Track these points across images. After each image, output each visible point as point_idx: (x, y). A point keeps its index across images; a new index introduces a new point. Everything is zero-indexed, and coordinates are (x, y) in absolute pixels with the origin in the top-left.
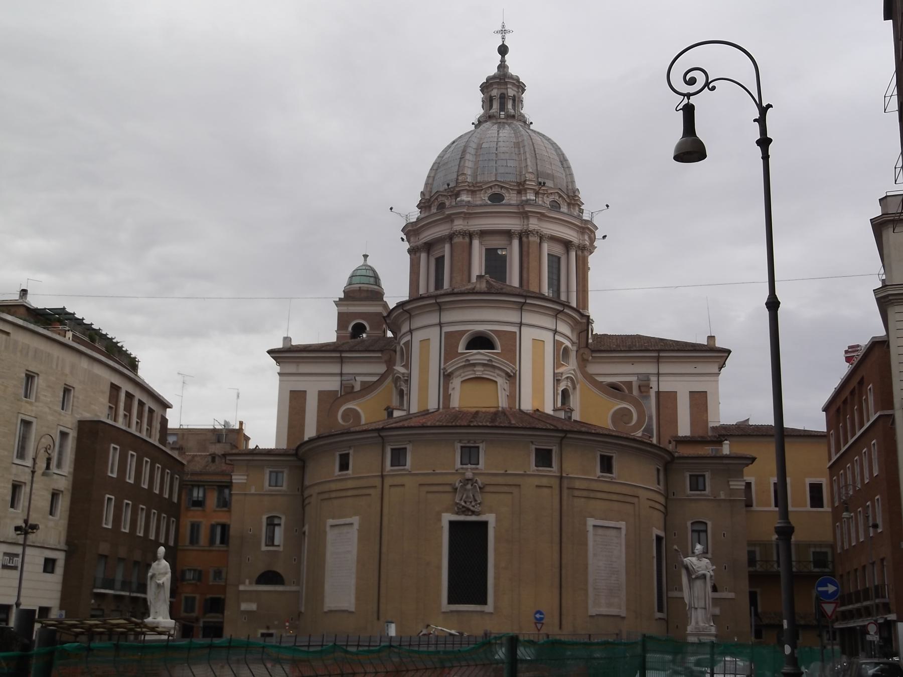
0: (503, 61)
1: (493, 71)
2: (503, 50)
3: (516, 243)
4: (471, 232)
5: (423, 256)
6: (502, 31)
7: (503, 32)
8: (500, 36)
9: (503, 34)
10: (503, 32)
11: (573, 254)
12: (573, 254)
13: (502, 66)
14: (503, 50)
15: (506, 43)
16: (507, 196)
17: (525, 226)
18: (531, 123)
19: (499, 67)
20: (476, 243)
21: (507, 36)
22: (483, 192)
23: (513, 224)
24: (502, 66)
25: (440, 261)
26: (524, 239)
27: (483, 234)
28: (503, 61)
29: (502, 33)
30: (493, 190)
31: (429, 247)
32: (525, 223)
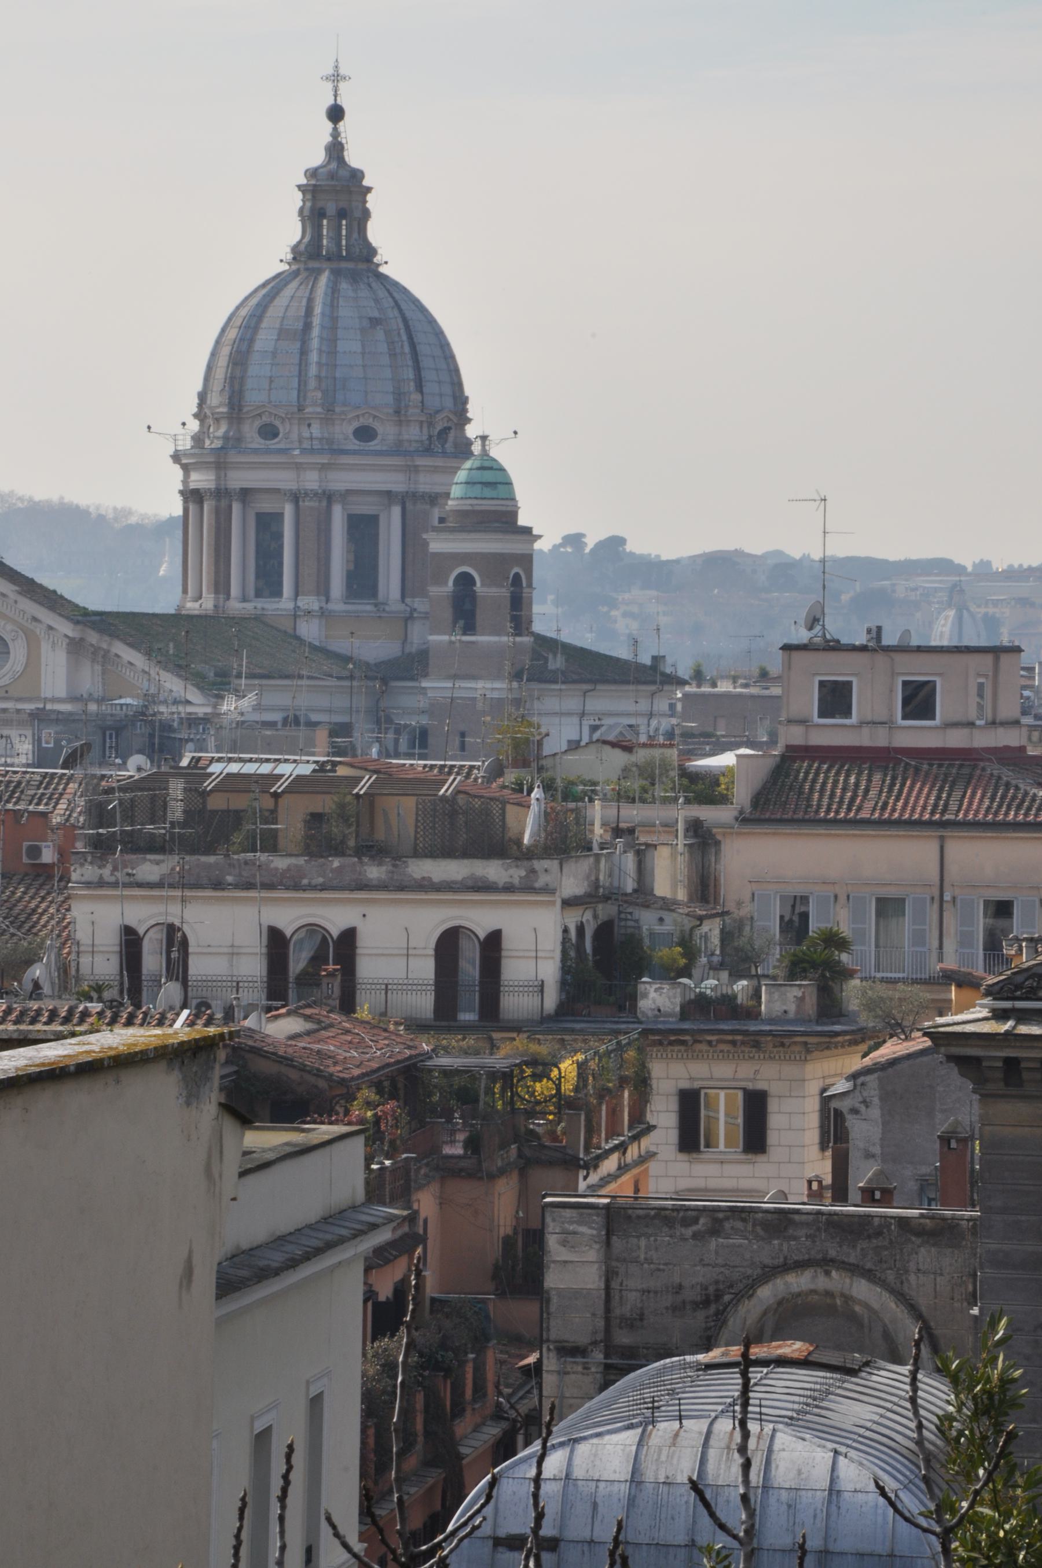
1: (317, 158)
2: (336, 114)
8: (329, 86)
13: (336, 149)
14: (336, 114)
15: (339, 102)
21: (342, 85)
24: (336, 149)
28: (335, 134)
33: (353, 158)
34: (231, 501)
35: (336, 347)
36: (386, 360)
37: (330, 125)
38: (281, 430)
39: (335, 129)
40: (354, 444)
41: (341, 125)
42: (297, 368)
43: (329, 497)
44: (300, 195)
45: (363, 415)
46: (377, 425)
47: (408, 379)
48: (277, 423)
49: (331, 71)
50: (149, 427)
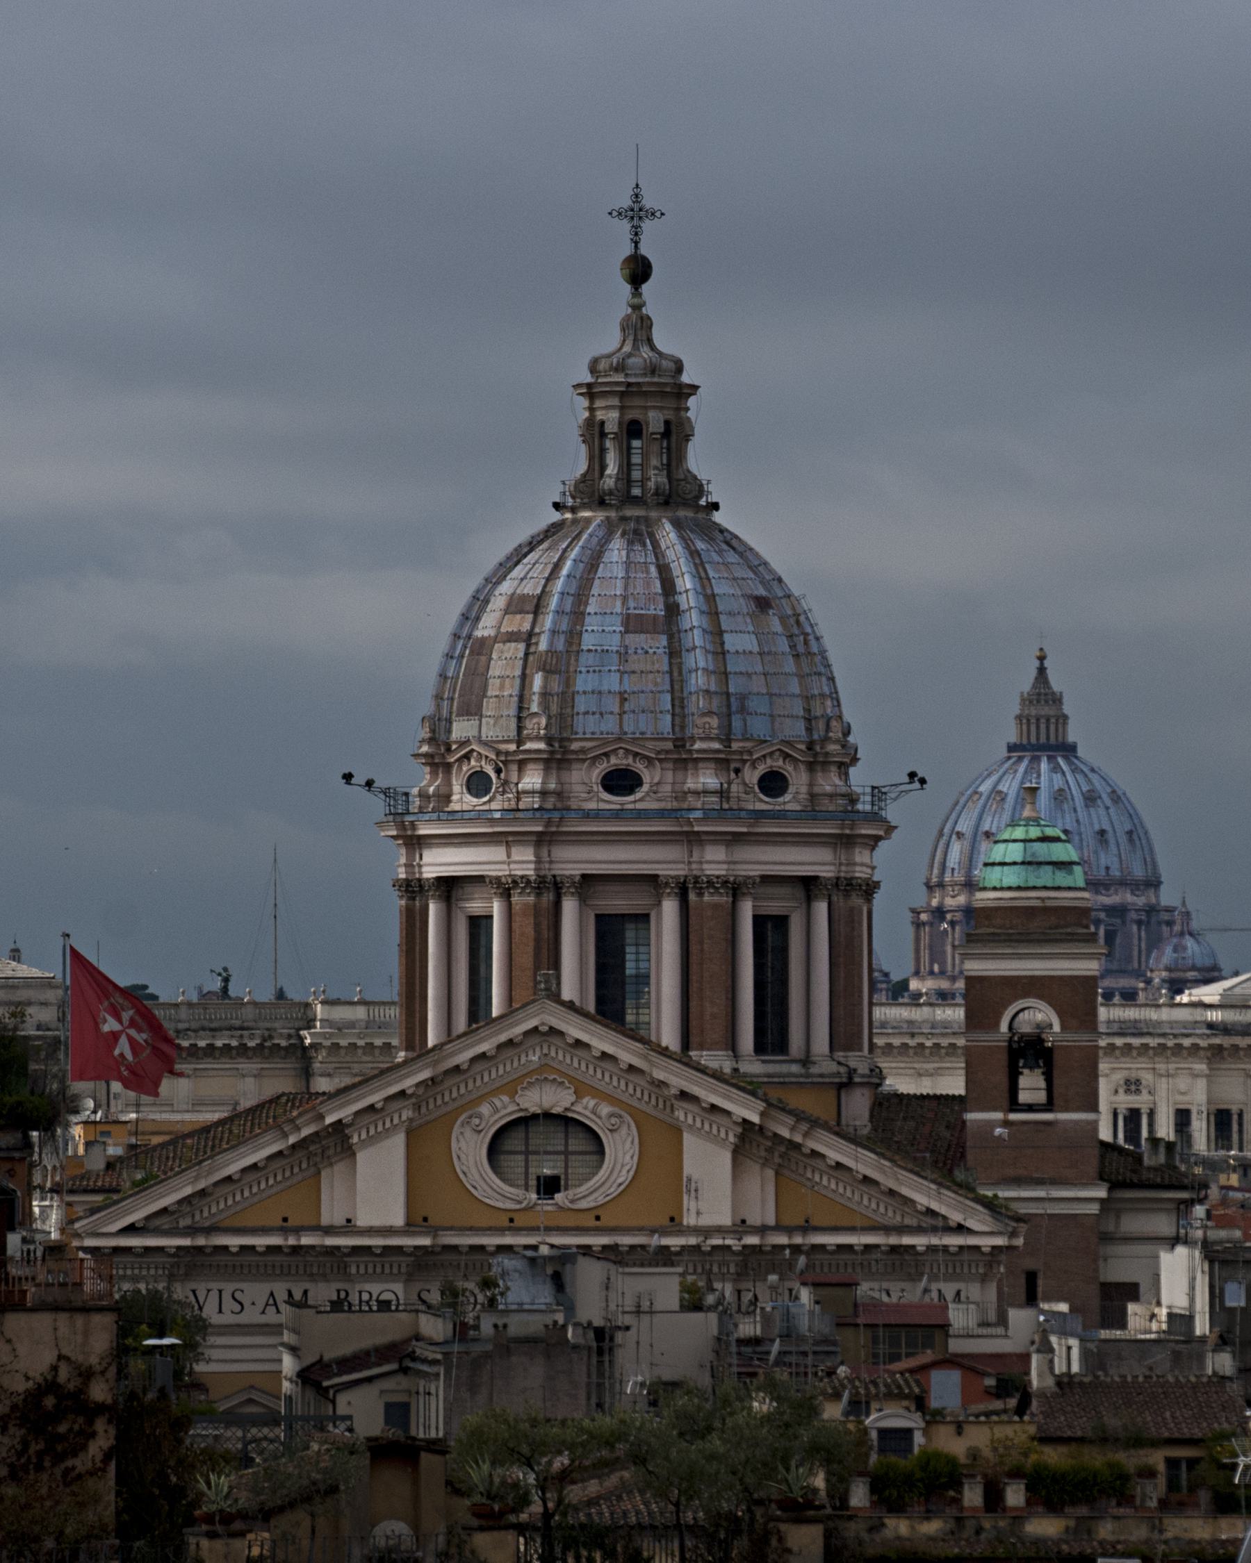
3: (670, 908)
4: (558, 879)
5: (434, 910)
7: (637, 213)
8: (625, 226)
9: (636, 207)
11: (821, 909)
12: (821, 908)
14: (638, 271)
15: (644, 250)
16: (648, 777)
17: (694, 866)
18: (716, 506)
20: (569, 907)
21: (647, 225)
22: (586, 764)
25: (479, 925)
26: (692, 897)
27: (588, 882)
28: (637, 308)
30: (613, 760)
31: (449, 887)
32: (695, 858)
35: (723, 644)
36: (790, 665)
37: (627, 288)
38: (646, 777)
40: (764, 803)
41: (645, 288)
42: (667, 677)
43: (736, 889)
45: (771, 754)
46: (788, 769)
47: (822, 695)
48: (639, 767)
50: (348, 777)
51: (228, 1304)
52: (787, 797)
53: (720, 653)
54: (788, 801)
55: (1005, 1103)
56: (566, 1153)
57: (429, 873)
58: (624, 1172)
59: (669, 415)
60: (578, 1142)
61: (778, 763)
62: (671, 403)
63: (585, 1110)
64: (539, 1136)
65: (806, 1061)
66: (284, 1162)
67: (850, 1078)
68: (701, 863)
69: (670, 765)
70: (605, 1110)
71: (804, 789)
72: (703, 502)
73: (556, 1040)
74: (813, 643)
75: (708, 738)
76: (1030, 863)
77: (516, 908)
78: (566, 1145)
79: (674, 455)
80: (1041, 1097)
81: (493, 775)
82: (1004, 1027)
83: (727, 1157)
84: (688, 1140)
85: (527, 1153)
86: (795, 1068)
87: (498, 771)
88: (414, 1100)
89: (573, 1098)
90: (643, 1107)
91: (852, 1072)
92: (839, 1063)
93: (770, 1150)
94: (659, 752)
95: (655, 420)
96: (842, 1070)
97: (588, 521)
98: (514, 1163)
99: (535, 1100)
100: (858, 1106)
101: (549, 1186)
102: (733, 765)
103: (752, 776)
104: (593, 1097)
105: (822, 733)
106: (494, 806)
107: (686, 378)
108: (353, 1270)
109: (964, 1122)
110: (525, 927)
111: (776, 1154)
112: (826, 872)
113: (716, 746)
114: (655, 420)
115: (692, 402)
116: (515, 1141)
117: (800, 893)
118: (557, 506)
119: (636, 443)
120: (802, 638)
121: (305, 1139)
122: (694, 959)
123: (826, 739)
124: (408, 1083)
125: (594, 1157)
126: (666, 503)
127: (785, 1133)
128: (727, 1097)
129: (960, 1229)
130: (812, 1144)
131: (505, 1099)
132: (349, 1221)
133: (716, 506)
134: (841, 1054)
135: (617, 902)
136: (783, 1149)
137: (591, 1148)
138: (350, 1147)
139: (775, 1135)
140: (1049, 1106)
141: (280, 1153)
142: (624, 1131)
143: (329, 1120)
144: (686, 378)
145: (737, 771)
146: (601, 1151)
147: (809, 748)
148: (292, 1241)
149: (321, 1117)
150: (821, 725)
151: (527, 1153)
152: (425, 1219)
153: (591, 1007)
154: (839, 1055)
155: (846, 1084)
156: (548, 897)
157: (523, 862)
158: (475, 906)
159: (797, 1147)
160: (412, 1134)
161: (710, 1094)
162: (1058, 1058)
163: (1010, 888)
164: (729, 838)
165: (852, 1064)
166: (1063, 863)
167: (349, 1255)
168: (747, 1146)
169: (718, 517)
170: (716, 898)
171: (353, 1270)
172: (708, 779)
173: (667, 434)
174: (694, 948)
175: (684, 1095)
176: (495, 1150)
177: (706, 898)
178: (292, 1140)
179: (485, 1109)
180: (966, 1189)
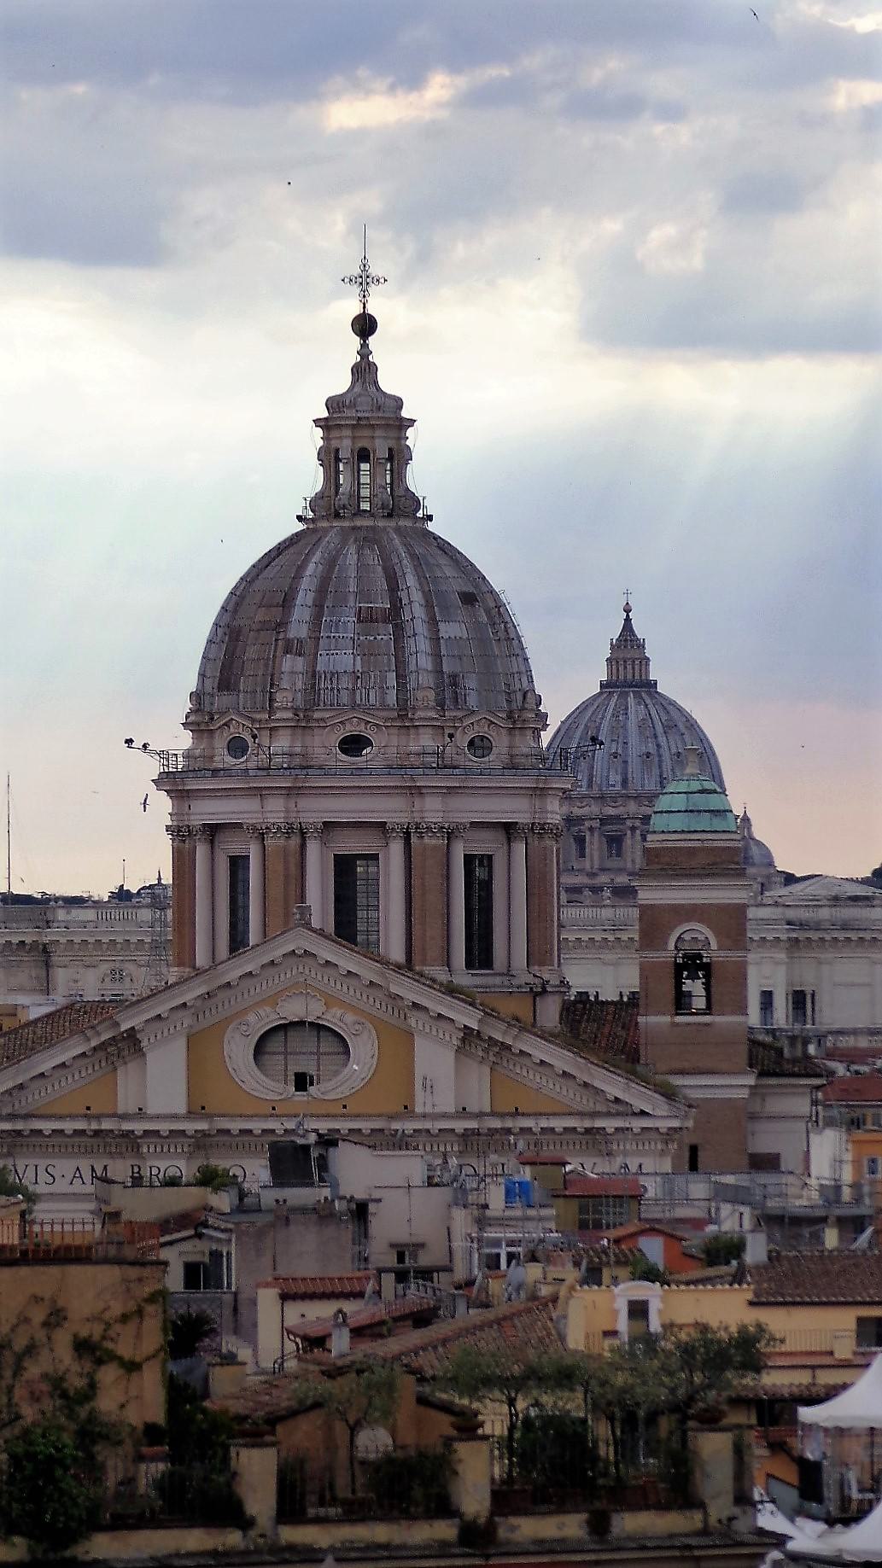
0: (364, 352)
1: (341, 383)
2: (365, 326)
3: (397, 848)
5: (201, 851)
6: (361, 284)
10: (364, 281)
11: (520, 849)
12: (520, 849)
13: (364, 370)
14: (365, 326)
15: (371, 310)
17: (415, 815)
18: (430, 518)
19: (356, 370)
20: (313, 848)
21: (372, 289)
23: (391, 810)
24: (364, 370)
25: (238, 865)
26: (414, 839)
28: (364, 352)
29: (361, 277)
31: (213, 831)
33: (388, 382)
34: (304, 840)
37: (356, 341)
39: (364, 345)
40: (472, 760)
43: (451, 834)
44: (319, 432)
46: (492, 734)
49: (357, 271)
50: (129, 742)
51: (43, 1177)
52: (492, 757)
53: (436, 640)
54: (493, 759)
55: (672, 1009)
56: (318, 1053)
57: (196, 821)
58: (366, 1069)
59: (392, 443)
60: (327, 1045)
61: (483, 730)
62: (393, 434)
63: (332, 1019)
64: (295, 1039)
65: (508, 974)
66: (87, 1061)
67: (544, 988)
68: (422, 811)
69: (395, 731)
70: (350, 1018)
71: (505, 750)
72: (420, 514)
73: (310, 961)
74: (511, 630)
75: (427, 708)
76: (691, 811)
77: (269, 849)
78: (319, 1047)
79: (396, 476)
80: (699, 1003)
81: (250, 740)
82: (671, 946)
83: (449, 1056)
84: (419, 1042)
85: (286, 1053)
86: (498, 980)
87: (254, 737)
88: (193, 1010)
89: (324, 1008)
90: (380, 1014)
91: (545, 984)
92: (534, 976)
93: (486, 1051)
94: (387, 720)
95: (381, 449)
96: (537, 981)
97: (326, 531)
98: (275, 1062)
99: (293, 1010)
100: (550, 1014)
101: (302, 1082)
102: (447, 731)
103: (463, 740)
104: (340, 1008)
105: (520, 704)
106: (250, 765)
107: (405, 413)
108: (145, 1150)
109: (637, 1023)
110: (276, 866)
111: (491, 1054)
112: (523, 818)
113: (433, 714)
114: (381, 449)
115: (410, 432)
116: (275, 1044)
117: (501, 836)
118: (299, 518)
119: (365, 466)
120: (502, 625)
121: (103, 1043)
122: (416, 892)
123: (523, 709)
124: (188, 997)
125: (343, 1057)
126: (390, 515)
127: (498, 1037)
128: (451, 1007)
129: (643, 1113)
130: (520, 1045)
131: (268, 1009)
132: (140, 1109)
133: (430, 518)
134: (536, 967)
135: (352, 844)
136: (497, 1049)
137: (341, 1050)
138: (141, 1050)
139: (490, 1038)
140: (709, 1010)
141: (84, 1054)
142: (365, 1035)
143: (124, 1027)
144: (405, 413)
145: (451, 736)
146: (347, 1052)
147: (509, 717)
148: (94, 1126)
149: (117, 1024)
150: (519, 696)
151: (286, 1053)
152: (203, 1108)
153: (330, 928)
154: (535, 969)
155: (539, 992)
156: (295, 841)
157: (275, 811)
158: (236, 848)
159: (509, 1048)
160: (192, 1041)
161: (438, 1004)
162: (715, 971)
163: (675, 832)
164: (445, 791)
165: (546, 977)
166: (718, 811)
167: (140, 1137)
168: (467, 1048)
169: (431, 527)
170: (434, 842)
171: (145, 1150)
172: (427, 740)
173: (391, 459)
174: (415, 882)
175: (415, 1005)
176: (259, 1050)
177: (426, 840)
178: (94, 1043)
179: (251, 1018)
180: (645, 1081)
